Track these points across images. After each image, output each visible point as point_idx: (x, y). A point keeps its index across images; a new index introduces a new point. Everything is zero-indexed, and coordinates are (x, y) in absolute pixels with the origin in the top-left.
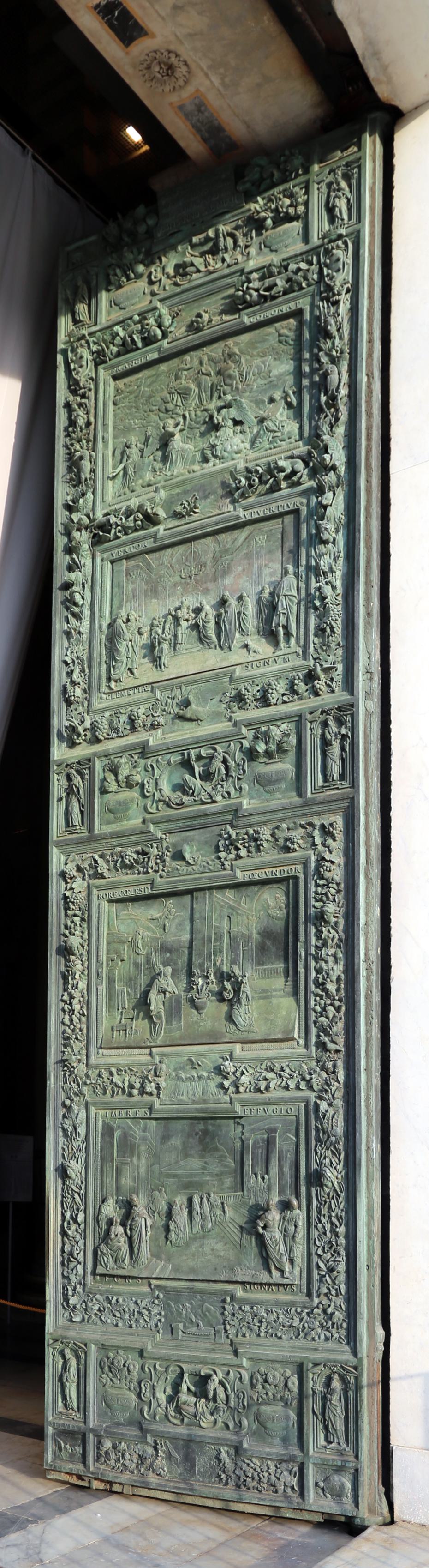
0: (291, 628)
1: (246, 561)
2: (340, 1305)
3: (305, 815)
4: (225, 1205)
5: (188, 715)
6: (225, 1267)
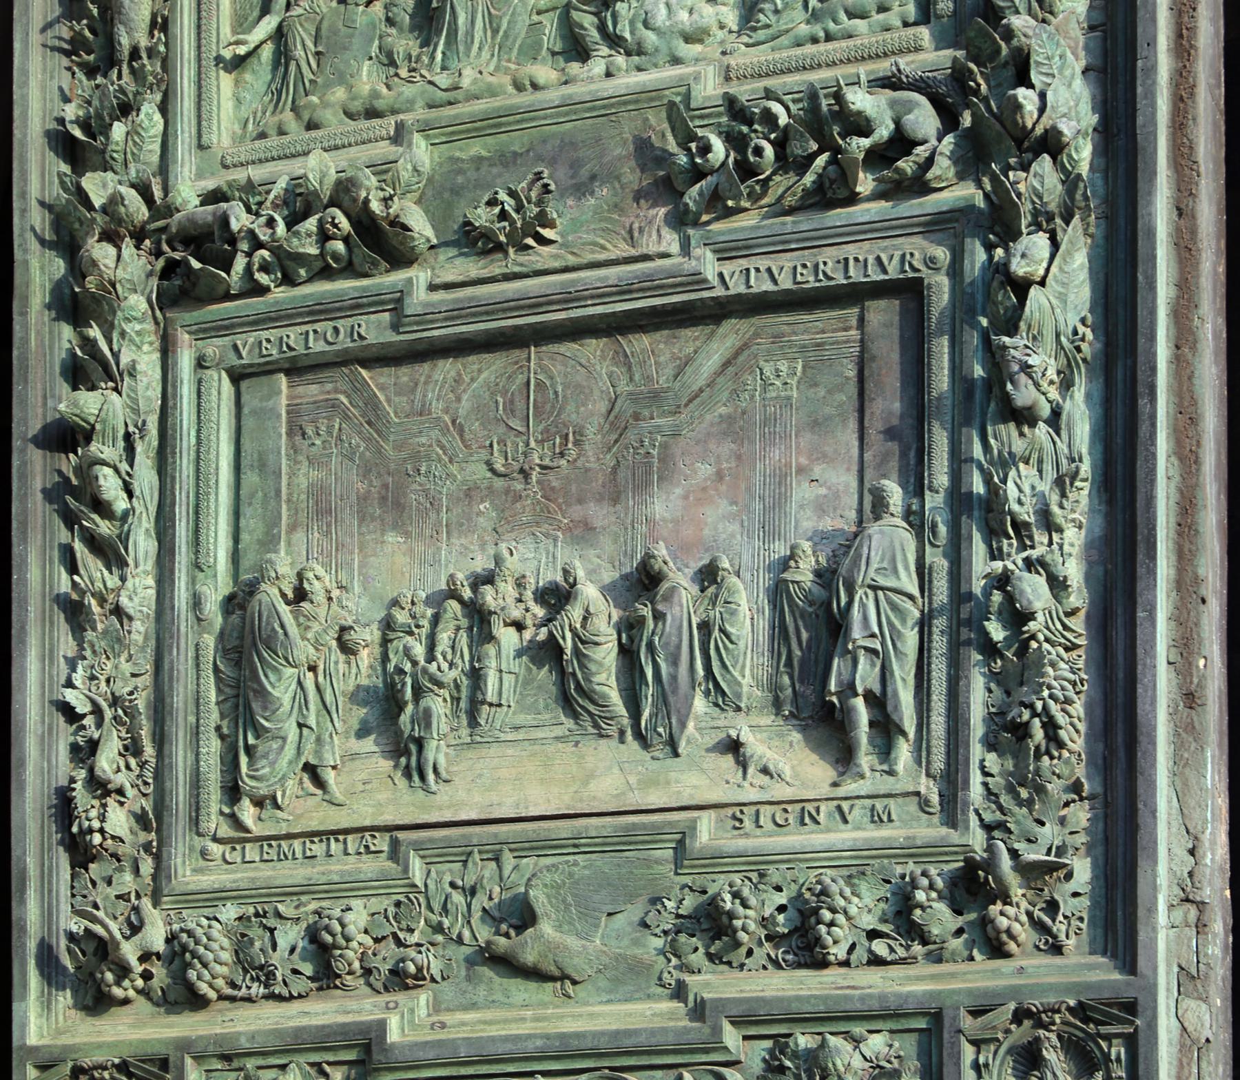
0: (897, 707)
1: (727, 447)
5: (529, 957)
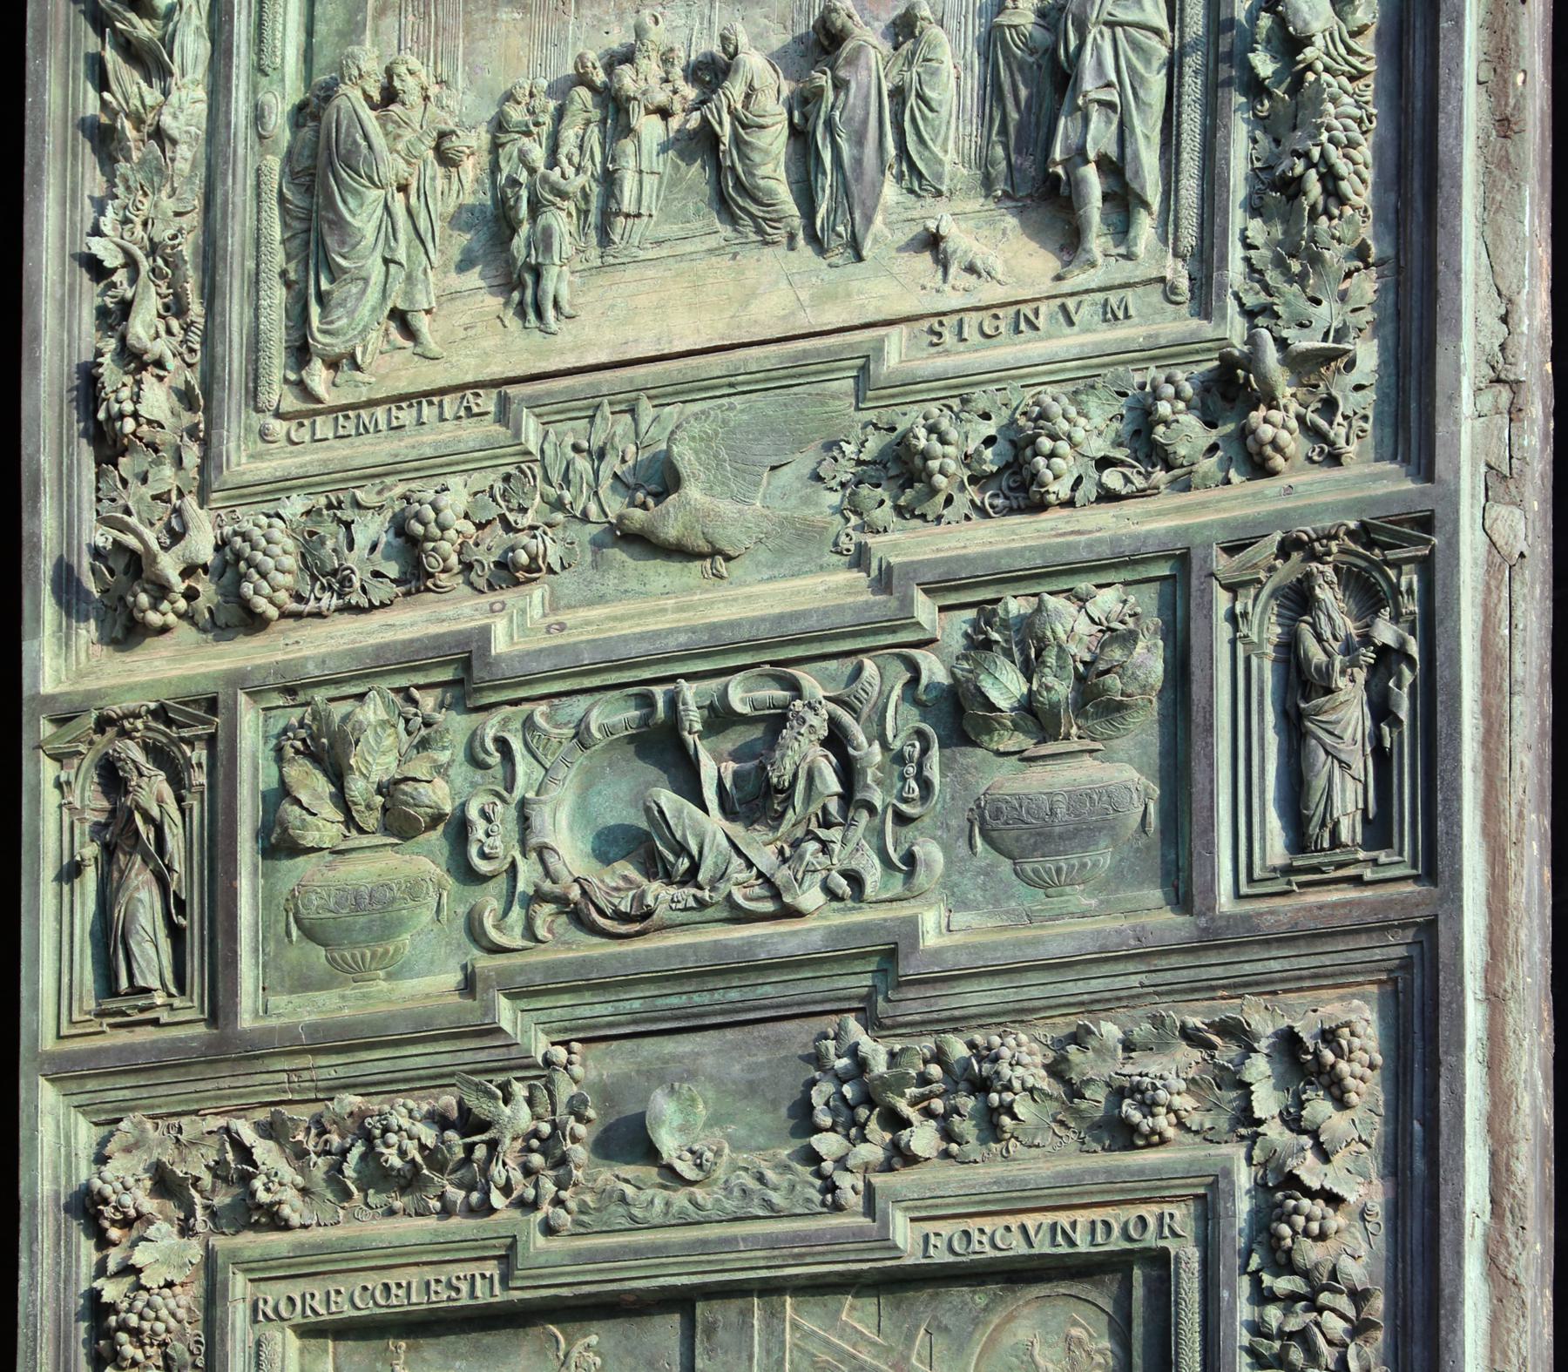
0: (1137, 173)
3: (1204, 989)
5: (671, 531)
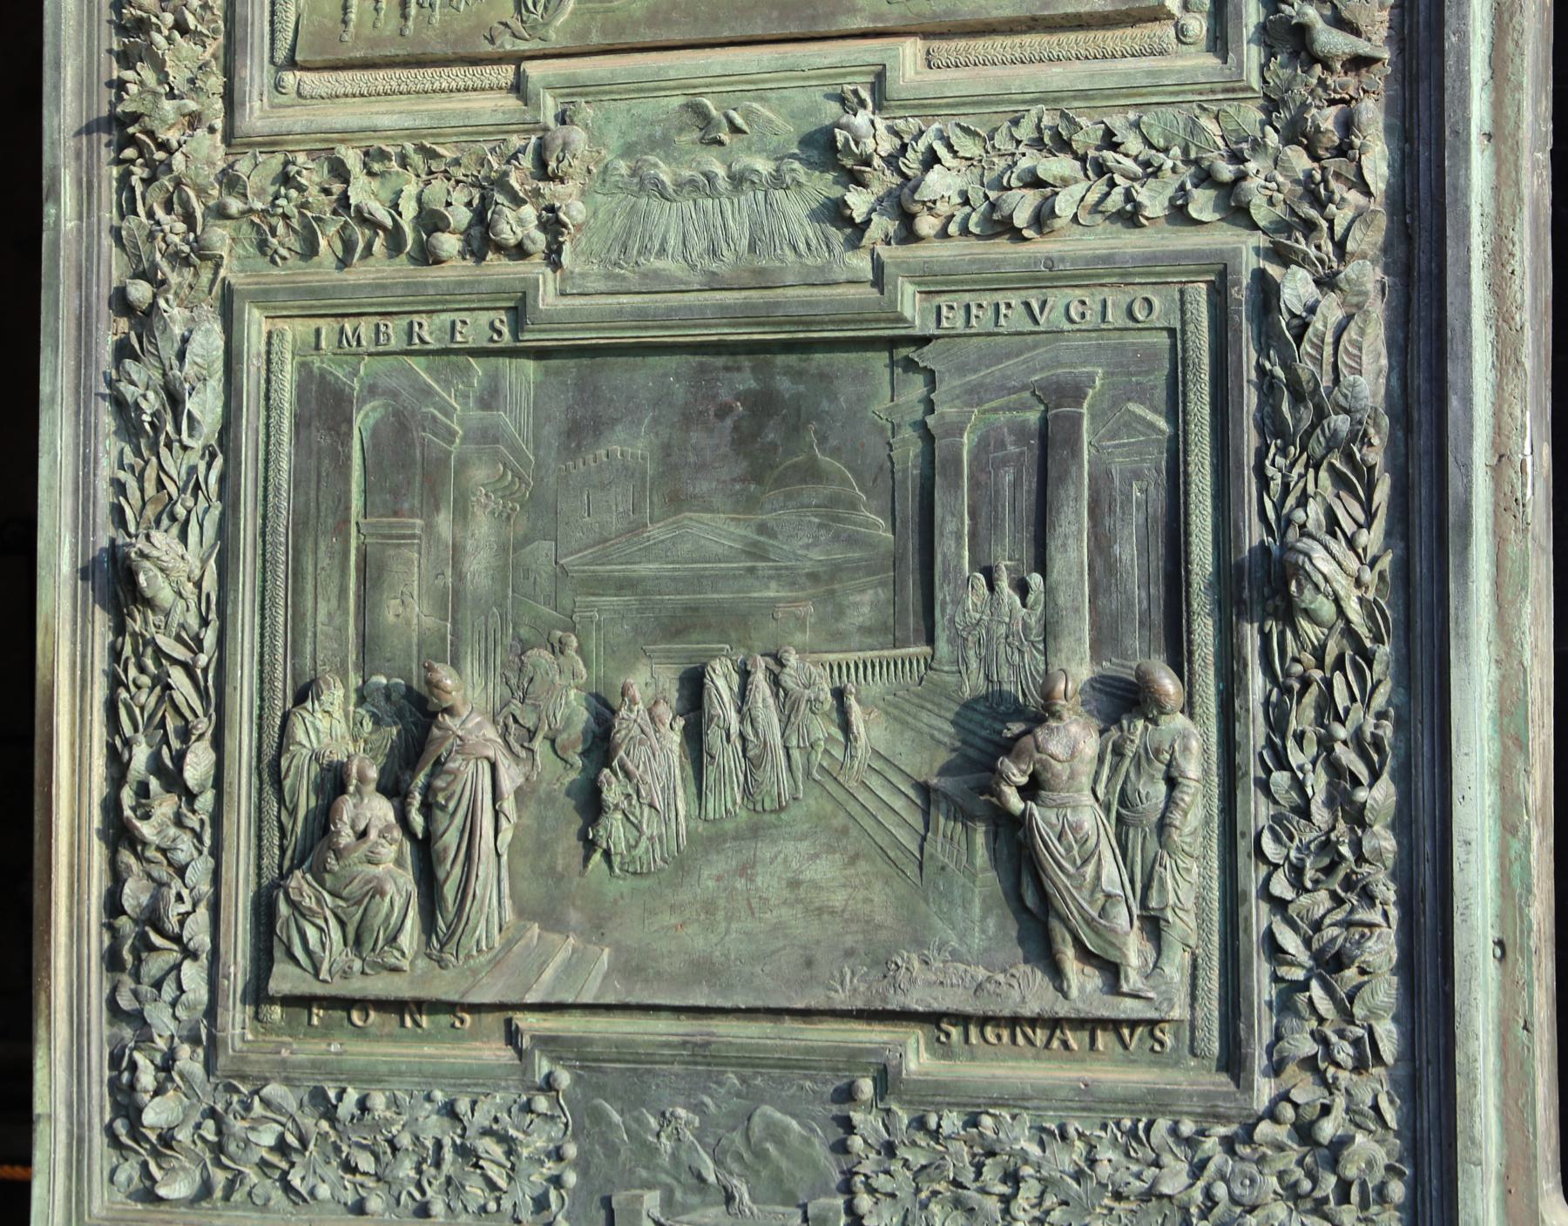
2: (1375, 1107)
4: (852, 701)
6: (849, 953)
